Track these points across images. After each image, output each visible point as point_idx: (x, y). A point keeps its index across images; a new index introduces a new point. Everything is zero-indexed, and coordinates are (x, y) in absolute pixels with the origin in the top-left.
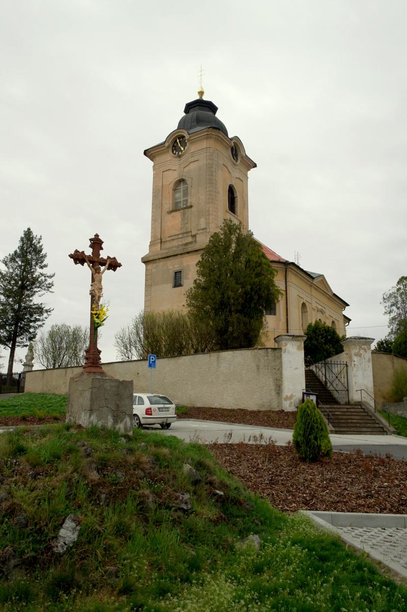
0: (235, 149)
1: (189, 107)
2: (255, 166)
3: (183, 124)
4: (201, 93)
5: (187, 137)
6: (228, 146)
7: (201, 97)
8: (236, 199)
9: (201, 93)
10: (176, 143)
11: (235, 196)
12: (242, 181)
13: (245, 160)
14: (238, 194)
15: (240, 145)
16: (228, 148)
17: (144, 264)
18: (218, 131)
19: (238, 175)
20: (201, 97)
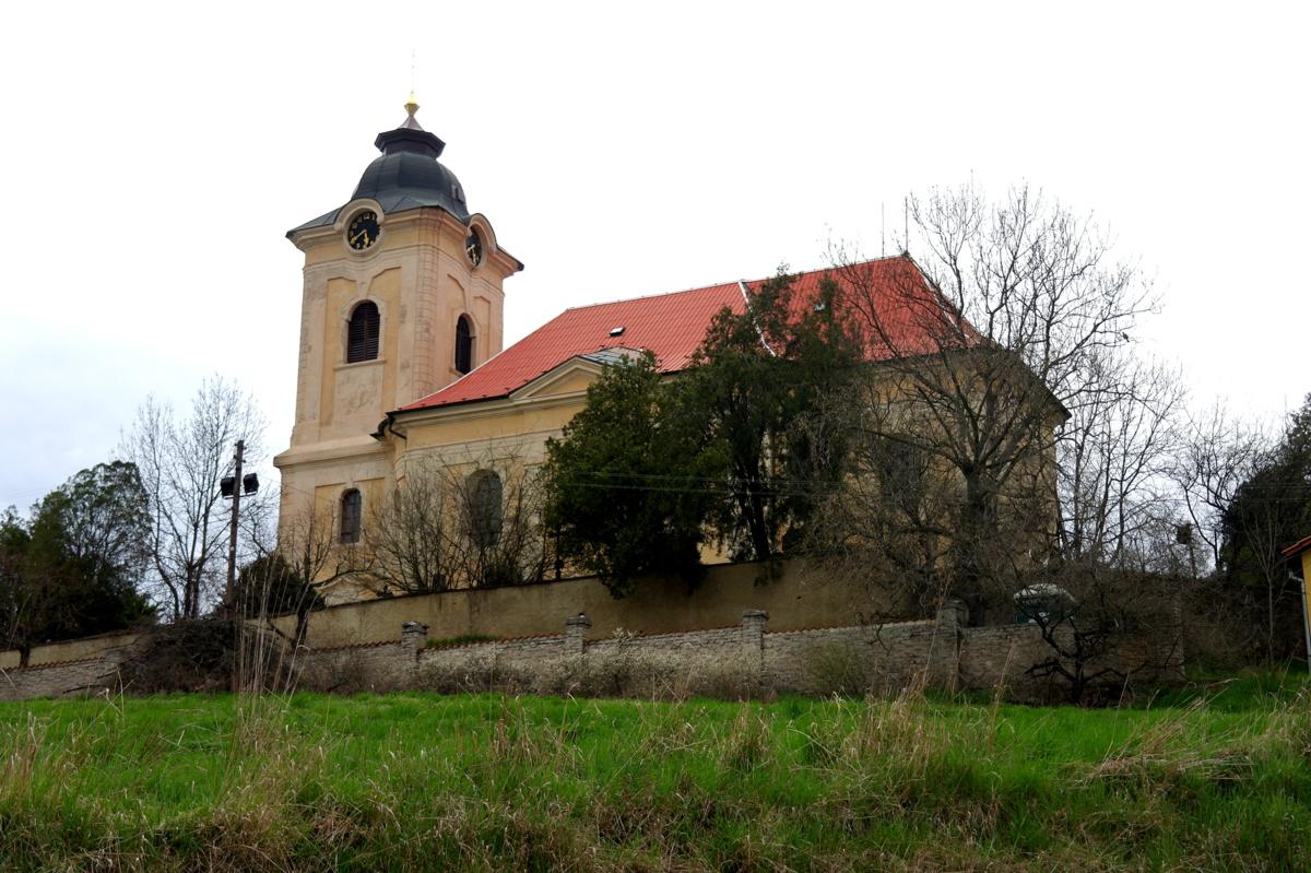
0: (477, 240)
1: (386, 141)
2: (520, 267)
3: (372, 183)
4: (412, 108)
5: (380, 218)
6: (460, 237)
7: (411, 119)
8: (473, 341)
9: (412, 108)
10: (359, 227)
11: (471, 335)
12: (489, 302)
13: (496, 259)
14: (478, 331)
15: (488, 232)
16: (460, 241)
17: (278, 470)
18: (440, 212)
19: (480, 291)
20: (411, 119)
